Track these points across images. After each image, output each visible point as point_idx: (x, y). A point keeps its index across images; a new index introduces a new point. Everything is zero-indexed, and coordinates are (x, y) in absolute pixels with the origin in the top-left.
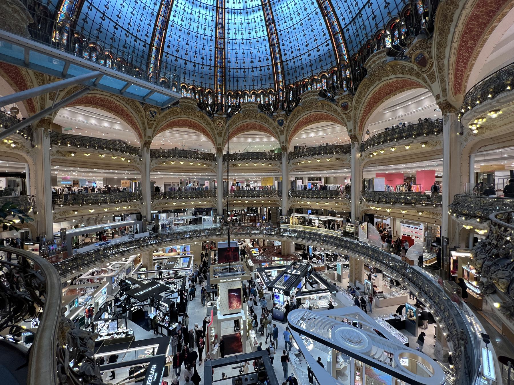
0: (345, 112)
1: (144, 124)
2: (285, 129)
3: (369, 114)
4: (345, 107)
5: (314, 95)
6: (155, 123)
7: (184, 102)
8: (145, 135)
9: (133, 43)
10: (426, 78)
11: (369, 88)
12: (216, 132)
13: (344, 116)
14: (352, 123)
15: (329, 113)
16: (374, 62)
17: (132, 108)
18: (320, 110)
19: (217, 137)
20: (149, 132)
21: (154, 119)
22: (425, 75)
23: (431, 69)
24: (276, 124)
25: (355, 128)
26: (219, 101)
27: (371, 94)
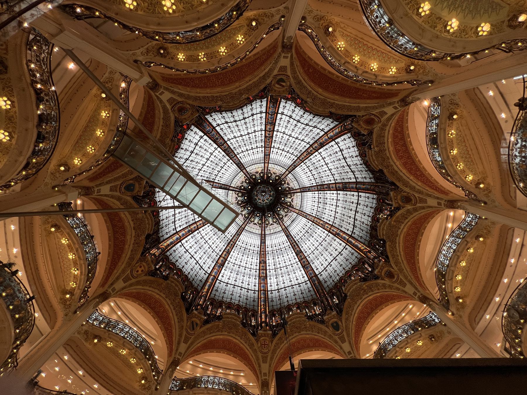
0: (394, 280)
1: (180, 335)
2: (344, 333)
3: (418, 270)
4: (390, 275)
5: (355, 284)
6: (193, 337)
7: (228, 318)
9: (198, 269)
10: (420, 205)
11: (396, 246)
12: (260, 355)
13: (396, 285)
14: (408, 286)
15: (380, 291)
16: (383, 229)
17: (177, 315)
18: (370, 294)
19: (262, 364)
20: (183, 347)
21: (193, 332)
22: (418, 205)
23: (415, 197)
24: (330, 331)
25: (416, 289)
26: (263, 320)
27: (401, 251)
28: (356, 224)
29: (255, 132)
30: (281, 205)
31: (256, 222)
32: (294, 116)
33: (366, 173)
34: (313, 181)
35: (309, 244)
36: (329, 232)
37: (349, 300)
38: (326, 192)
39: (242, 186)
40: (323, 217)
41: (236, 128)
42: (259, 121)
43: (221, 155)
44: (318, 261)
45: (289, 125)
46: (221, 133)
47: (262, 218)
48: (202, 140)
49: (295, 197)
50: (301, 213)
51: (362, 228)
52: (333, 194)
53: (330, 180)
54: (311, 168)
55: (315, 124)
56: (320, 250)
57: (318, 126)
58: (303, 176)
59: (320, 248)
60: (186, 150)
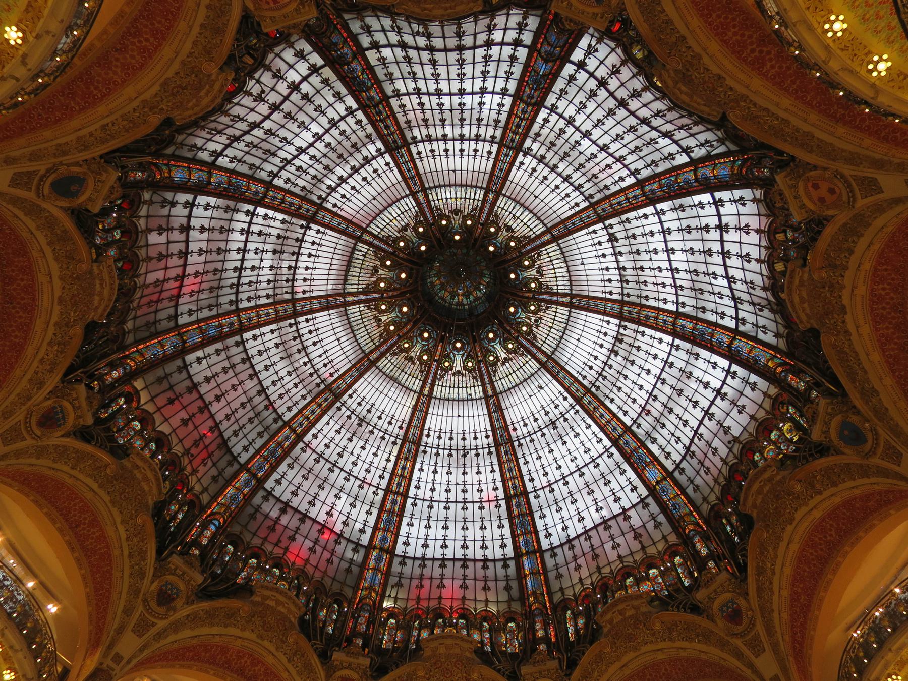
1: (128, 612)
8: (110, 647)
28: (693, 448)
29: (483, 91)
30: (501, 324)
31: (415, 352)
32: (613, 84)
33: (772, 316)
34: (615, 287)
35: (547, 458)
36: (615, 442)
37: (603, 645)
38: (641, 329)
39: (402, 238)
40: (612, 396)
41: (429, 70)
42: (504, 67)
43: (361, 134)
44: (557, 516)
45: (591, 106)
46: (380, 72)
47: (436, 346)
48: (315, 80)
49: (547, 317)
50: (552, 366)
51: (707, 463)
52: (661, 341)
53: (665, 301)
54: (622, 245)
55: (669, 127)
56: (572, 486)
57: (678, 135)
58: (590, 260)
59: (575, 482)
60: (260, 99)
